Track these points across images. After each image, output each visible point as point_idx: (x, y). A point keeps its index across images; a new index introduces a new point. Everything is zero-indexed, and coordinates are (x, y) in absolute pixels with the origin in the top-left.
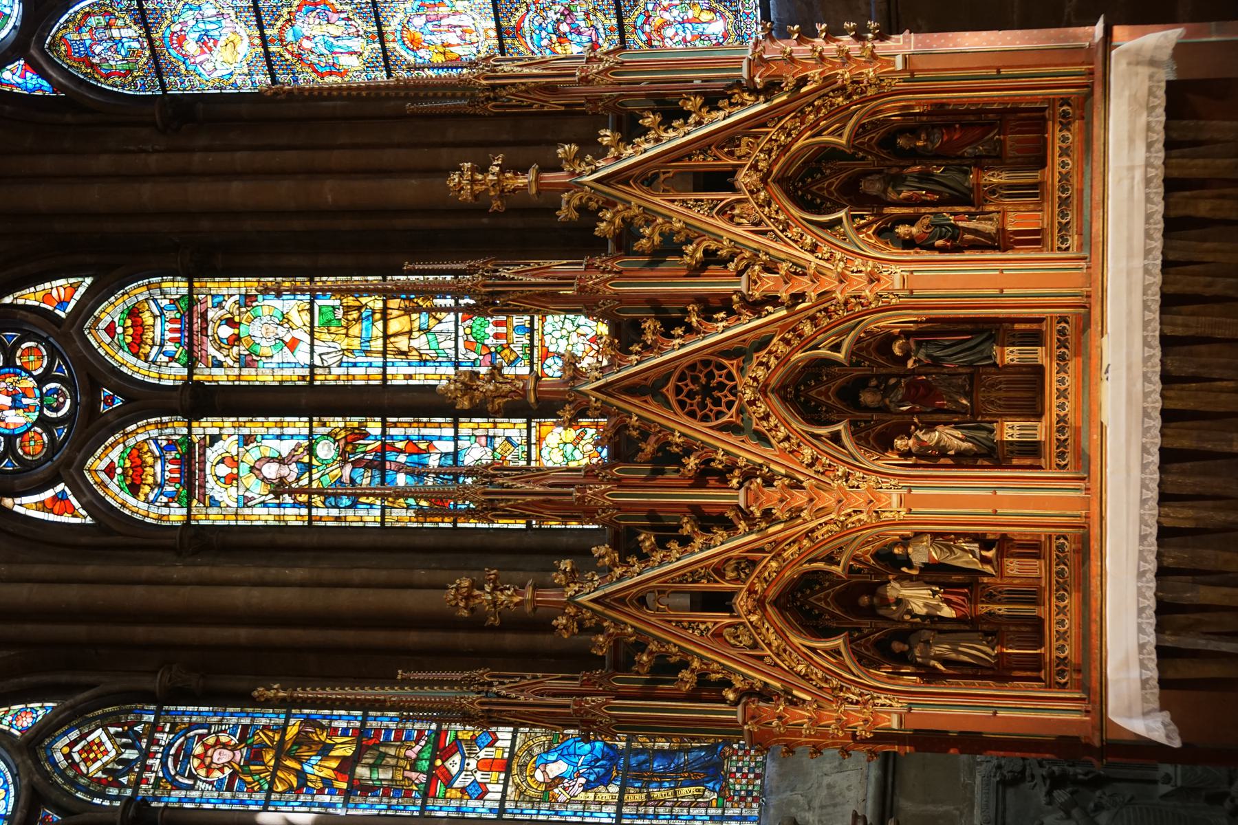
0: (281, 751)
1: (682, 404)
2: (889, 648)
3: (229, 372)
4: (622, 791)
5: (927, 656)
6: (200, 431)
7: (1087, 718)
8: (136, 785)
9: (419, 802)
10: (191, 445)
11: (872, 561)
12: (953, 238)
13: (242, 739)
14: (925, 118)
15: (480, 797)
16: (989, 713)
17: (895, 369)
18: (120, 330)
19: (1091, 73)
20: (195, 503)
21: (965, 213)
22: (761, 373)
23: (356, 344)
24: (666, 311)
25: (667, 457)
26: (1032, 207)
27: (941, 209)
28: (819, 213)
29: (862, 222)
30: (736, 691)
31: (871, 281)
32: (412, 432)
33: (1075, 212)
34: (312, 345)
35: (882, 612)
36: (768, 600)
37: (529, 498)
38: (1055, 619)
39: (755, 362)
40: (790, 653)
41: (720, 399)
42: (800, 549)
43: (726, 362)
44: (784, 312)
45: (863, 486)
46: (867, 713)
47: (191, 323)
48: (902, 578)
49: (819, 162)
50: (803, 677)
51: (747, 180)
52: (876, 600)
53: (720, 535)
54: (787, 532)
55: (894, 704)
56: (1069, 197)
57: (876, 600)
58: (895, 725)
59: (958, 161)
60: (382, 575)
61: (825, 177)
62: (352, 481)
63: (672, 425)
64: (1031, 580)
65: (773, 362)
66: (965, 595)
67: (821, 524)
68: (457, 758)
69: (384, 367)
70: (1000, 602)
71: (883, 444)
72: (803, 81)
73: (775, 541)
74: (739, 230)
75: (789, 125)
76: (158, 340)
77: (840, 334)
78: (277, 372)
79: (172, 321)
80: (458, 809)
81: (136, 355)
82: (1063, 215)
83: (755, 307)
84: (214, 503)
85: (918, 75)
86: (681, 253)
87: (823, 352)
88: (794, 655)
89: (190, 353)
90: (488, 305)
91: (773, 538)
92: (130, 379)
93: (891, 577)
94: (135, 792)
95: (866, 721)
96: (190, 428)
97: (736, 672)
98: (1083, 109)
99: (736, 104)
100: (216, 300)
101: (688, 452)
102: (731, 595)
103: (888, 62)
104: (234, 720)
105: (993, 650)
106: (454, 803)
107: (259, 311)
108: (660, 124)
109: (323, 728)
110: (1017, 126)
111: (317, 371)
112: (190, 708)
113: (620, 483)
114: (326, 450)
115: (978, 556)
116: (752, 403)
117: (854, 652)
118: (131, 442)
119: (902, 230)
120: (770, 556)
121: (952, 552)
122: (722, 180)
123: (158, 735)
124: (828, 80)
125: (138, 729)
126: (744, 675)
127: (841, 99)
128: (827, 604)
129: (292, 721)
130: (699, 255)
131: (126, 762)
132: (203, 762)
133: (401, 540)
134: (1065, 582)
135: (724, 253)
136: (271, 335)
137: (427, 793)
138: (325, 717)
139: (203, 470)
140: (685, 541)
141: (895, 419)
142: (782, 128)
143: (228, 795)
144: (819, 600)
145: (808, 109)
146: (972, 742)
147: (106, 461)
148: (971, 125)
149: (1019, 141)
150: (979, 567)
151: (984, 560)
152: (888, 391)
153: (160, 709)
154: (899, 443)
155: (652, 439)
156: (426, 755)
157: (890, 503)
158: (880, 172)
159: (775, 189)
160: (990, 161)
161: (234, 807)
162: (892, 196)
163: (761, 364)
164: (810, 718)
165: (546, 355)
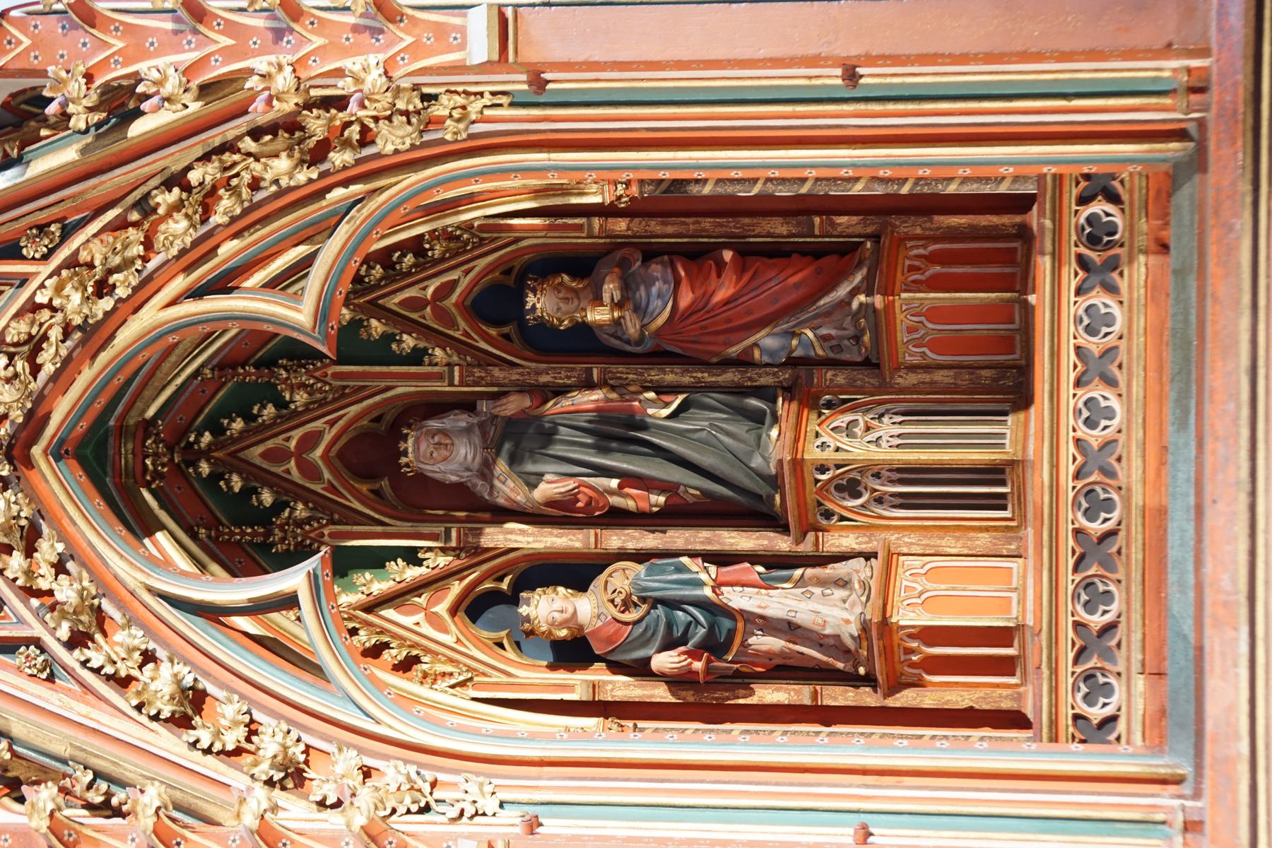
12: (713, 646)
14: (621, 225)
21: (752, 558)
26: (983, 541)
27: (678, 538)
29: (413, 573)
33: (1136, 589)
56: (1112, 533)
59: (730, 376)
61: (288, 417)
75: (97, 253)
82: (1095, 597)
85: (560, 83)
98: (1164, 216)
103: (441, 31)
110: (932, 259)
127: (282, 164)
142: (72, 263)
145: (166, 199)
148: (776, 252)
149: (935, 314)
158: (467, 405)
160: (841, 380)
162: (509, 489)
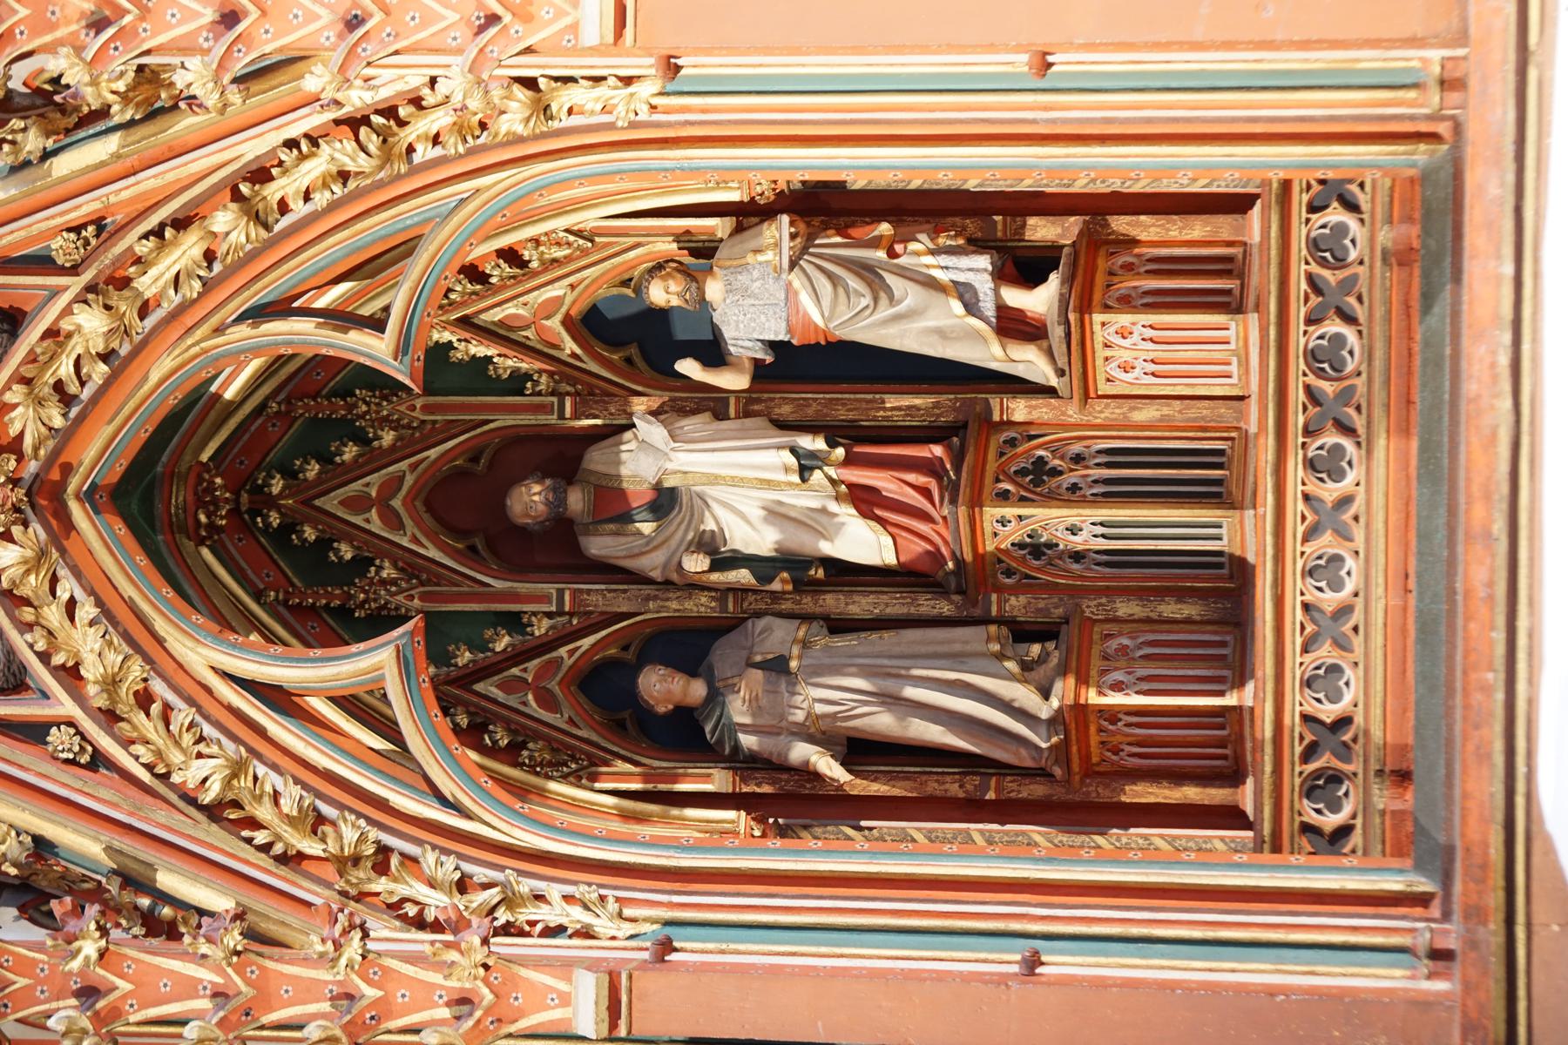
2: (632, 697)
7: (1441, 986)
11: (570, 346)
16: (1008, 960)
35: (599, 546)
36: (73, 484)
38: (1298, 555)
40: (167, 708)
42: (209, 256)
50: (213, 812)
52: (576, 500)
54: (150, 181)
55: (603, 924)
57: (576, 500)
64: (1202, 410)
66: (930, 467)
67: (291, 144)
70: (1074, 496)
73: (99, 223)
88: (183, 715)
91: (87, 206)
93: (639, 405)
95: (464, 1001)
105: (1046, 694)
115: (989, 308)
120: (76, 284)
128: (397, 524)
134: (1346, 396)
144: (359, 503)
150: (992, 354)
151: (1013, 326)
157: (574, 28)
164: (219, 995)
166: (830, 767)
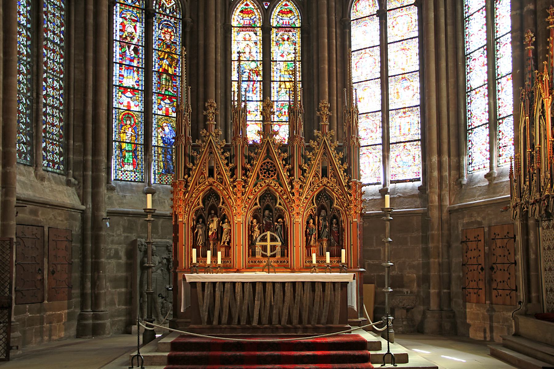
0: (169, 53)
1: (264, 163)
3: (275, 38)
4: (161, 147)
5: (198, 228)
6: (258, 30)
8: (161, 14)
9: (156, 92)
10: (254, 27)
12: (309, 234)
13: (172, 42)
15: (158, 109)
16: (184, 244)
17: (275, 219)
18: (286, 7)
19: (351, 268)
20: (238, 28)
22: (273, 184)
23: (282, 73)
24: (290, 159)
25: (250, 159)
27: (317, 231)
28: (316, 199)
30: (187, 178)
31: (297, 213)
32: (258, 89)
34: (282, 61)
35: (210, 216)
37: (238, 122)
39: (276, 183)
41: (266, 173)
43: (276, 175)
44: (289, 191)
45: (243, 212)
46: (182, 213)
47: (288, 27)
48: (219, 222)
49: (330, 199)
51: (325, 180)
53: (229, 174)
58: (179, 220)
60: (219, 81)
61: (326, 201)
62: (245, 72)
63: (259, 161)
65: (276, 188)
68: (169, 102)
69: (276, 81)
71: (255, 217)
72: (351, 195)
74: (311, 178)
76: (283, 18)
77: (284, 205)
78: (274, 52)
79: (289, 22)
80: (155, 102)
81: (279, 12)
83: (291, 183)
84: (238, 34)
86: (305, 163)
87: (279, 201)
89: (280, 27)
90: (291, 111)
92: (272, 10)
94: (157, 13)
95: (180, 212)
96: (259, 27)
97: (192, 178)
99: (345, 178)
100: (294, 35)
101: (251, 165)
102: (213, 177)
104: (178, 40)
106: (156, 102)
107: (291, 46)
108: (340, 157)
109: (176, 65)
111: (275, 62)
112: (181, 28)
113: (243, 147)
114: (253, 65)
116: (265, 182)
117: (199, 209)
118: (255, 11)
119: (311, 221)
121: (226, 234)
122: (325, 173)
123: (173, 19)
124: (351, 202)
125: (175, 13)
126: (191, 181)
129: (178, 56)
130: (305, 168)
131: (166, 10)
132: (166, 31)
133: (229, 86)
135: (305, 174)
136: (285, 50)
137: (159, 94)
138: (179, 65)
139: (247, 31)
140: (227, 165)
141: (261, 220)
143: (157, 39)
146: (176, 240)
147: (249, 4)
148: (339, 238)
149: (334, 250)
150: (222, 241)
151: (224, 243)
152: (269, 218)
153: (181, 19)
154: (255, 220)
155: (255, 155)
156: (169, 94)
158: (327, 215)
159: (322, 188)
161: (154, 41)
162: (321, 218)
163: (275, 185)
165: (279, 126)
166: (196, 231)
